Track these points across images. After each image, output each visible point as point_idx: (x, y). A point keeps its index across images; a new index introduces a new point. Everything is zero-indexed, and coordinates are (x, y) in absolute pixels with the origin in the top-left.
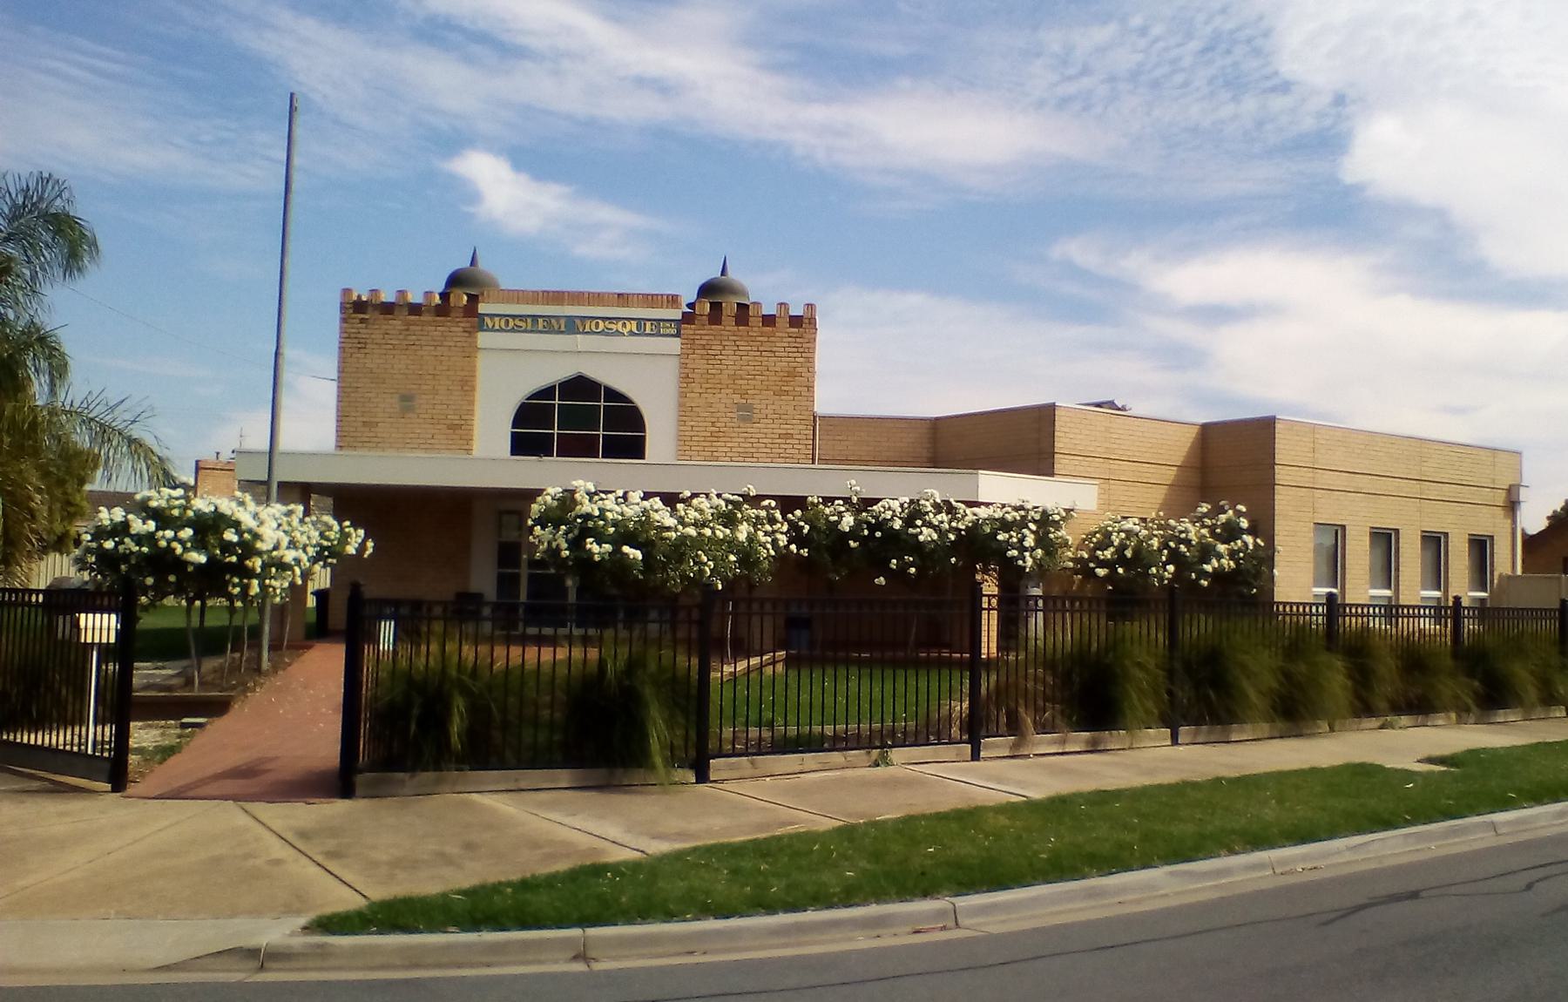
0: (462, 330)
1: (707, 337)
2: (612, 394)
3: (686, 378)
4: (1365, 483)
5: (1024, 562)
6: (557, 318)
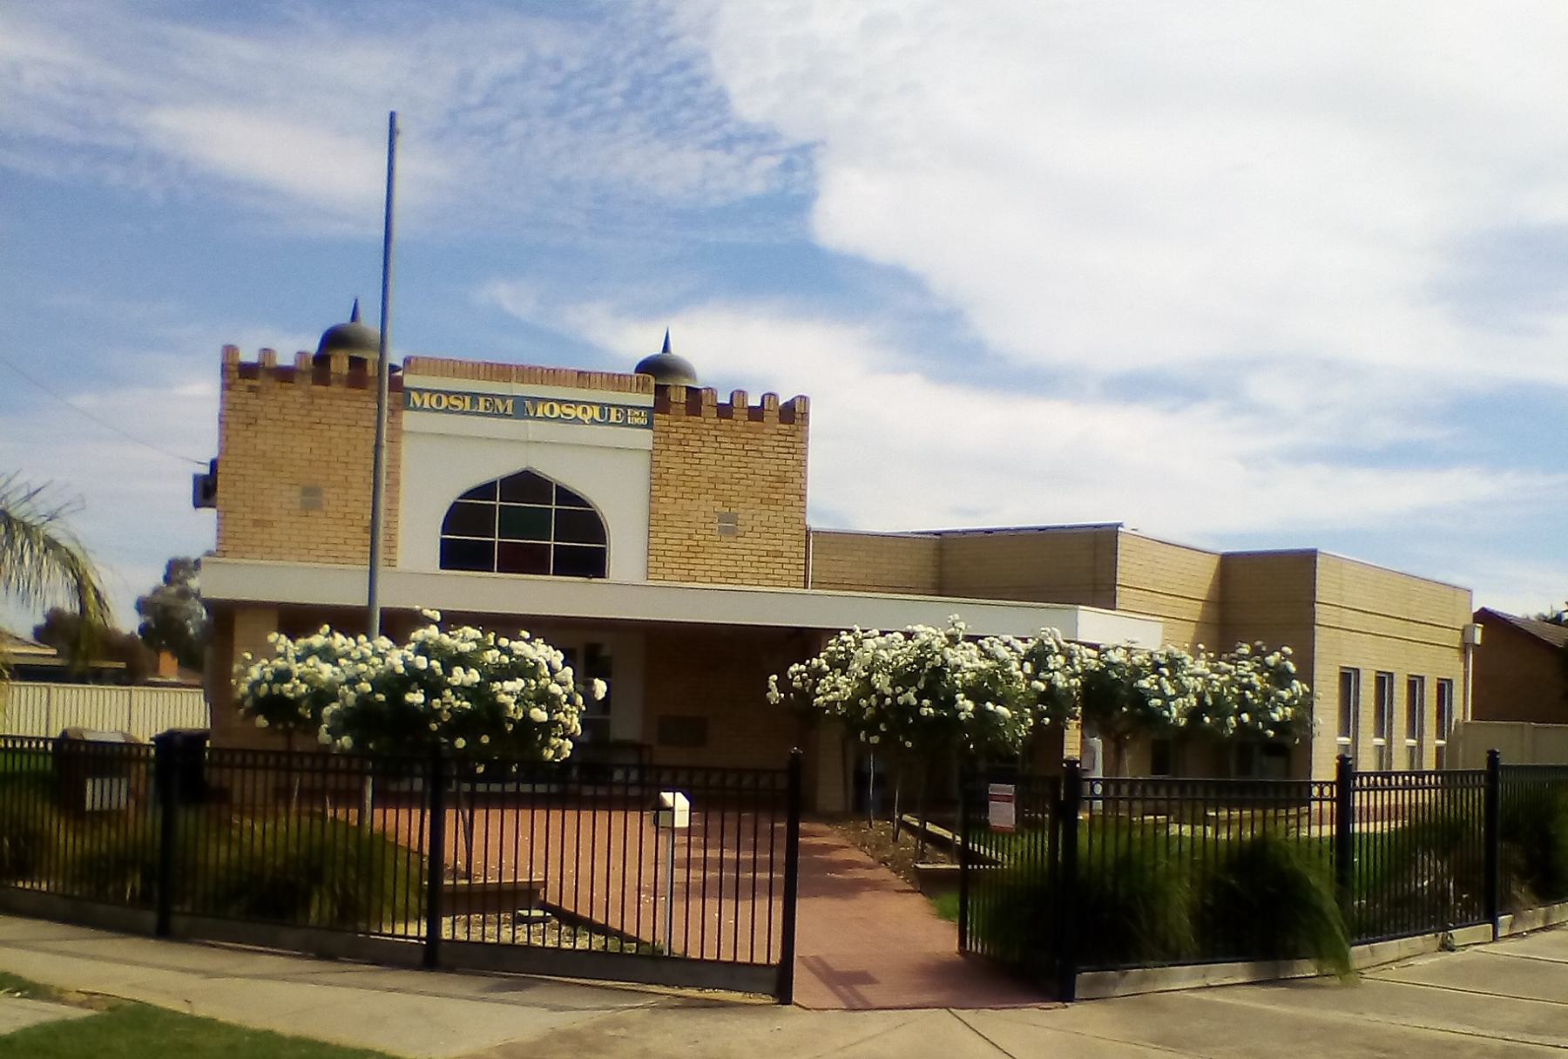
2: (566, 496)
3: (657, 479)
4: (1372, 623)
5: (1170, 713)
6: (503, 398)
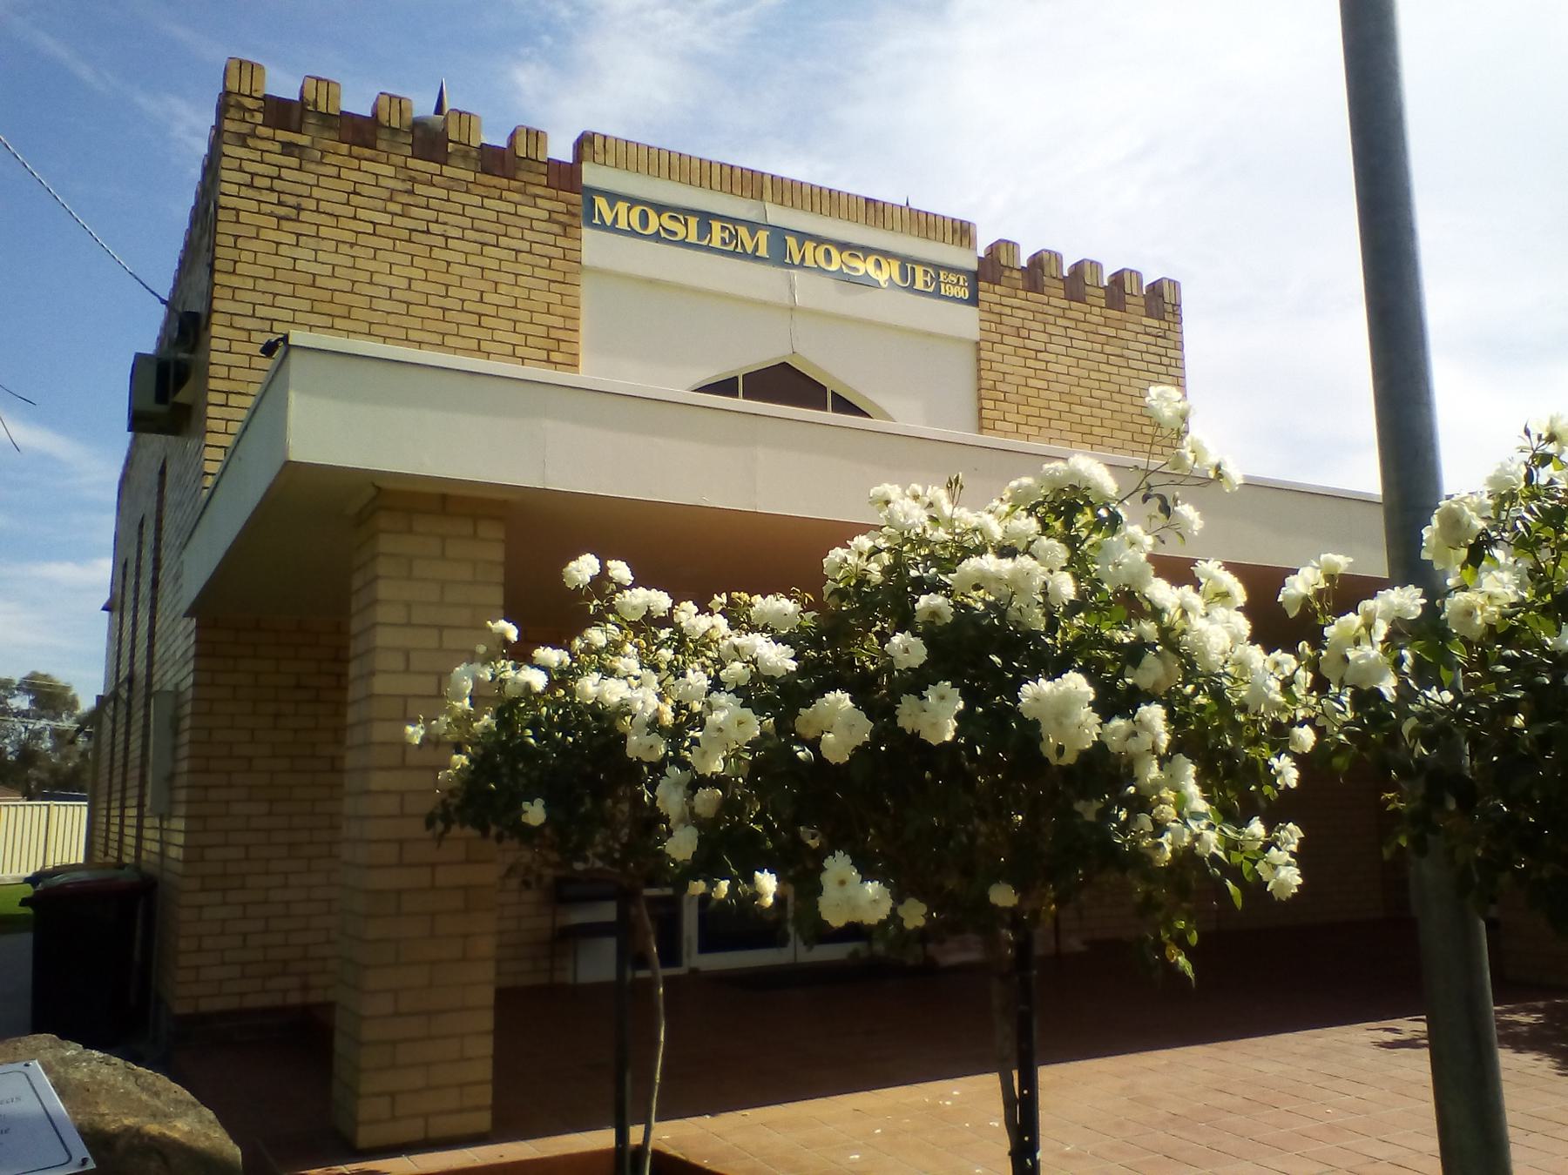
6: (753, 227)
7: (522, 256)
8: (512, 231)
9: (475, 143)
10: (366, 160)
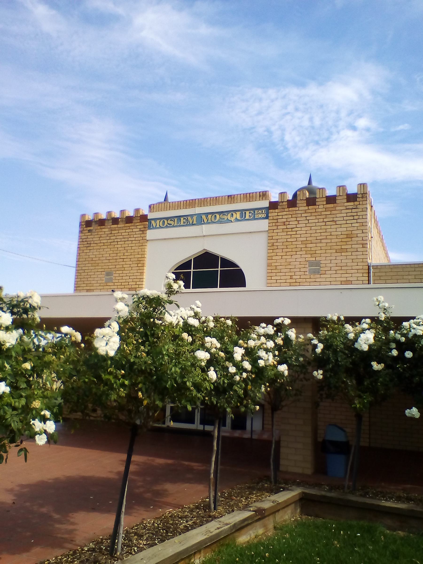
0: (138, 230)
1: (286, 217)
2: (226, 263)
6: (192, 216)
7: (133, 242)
8: (131, 236)
9: (124, 217)
10: (103, 229)
